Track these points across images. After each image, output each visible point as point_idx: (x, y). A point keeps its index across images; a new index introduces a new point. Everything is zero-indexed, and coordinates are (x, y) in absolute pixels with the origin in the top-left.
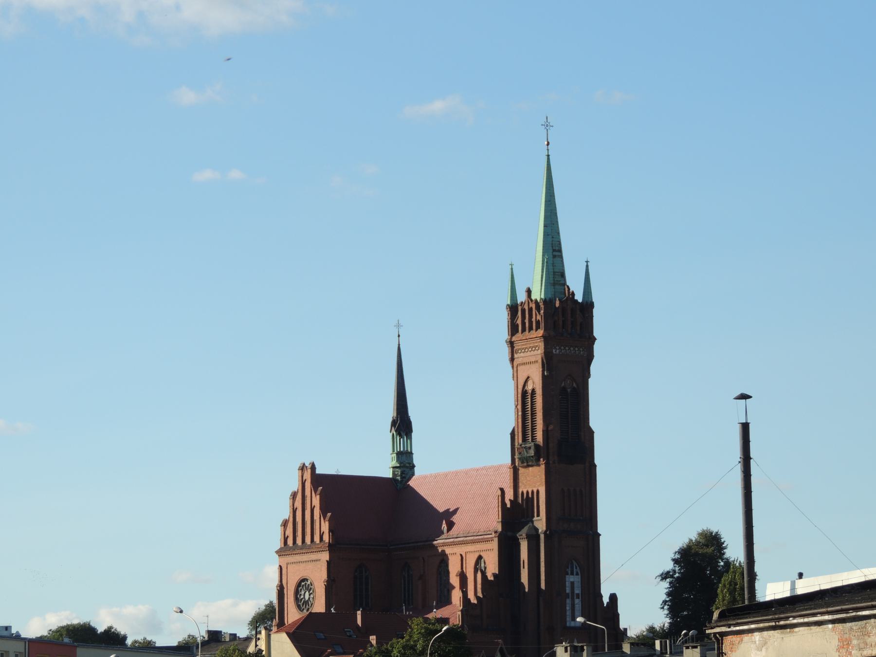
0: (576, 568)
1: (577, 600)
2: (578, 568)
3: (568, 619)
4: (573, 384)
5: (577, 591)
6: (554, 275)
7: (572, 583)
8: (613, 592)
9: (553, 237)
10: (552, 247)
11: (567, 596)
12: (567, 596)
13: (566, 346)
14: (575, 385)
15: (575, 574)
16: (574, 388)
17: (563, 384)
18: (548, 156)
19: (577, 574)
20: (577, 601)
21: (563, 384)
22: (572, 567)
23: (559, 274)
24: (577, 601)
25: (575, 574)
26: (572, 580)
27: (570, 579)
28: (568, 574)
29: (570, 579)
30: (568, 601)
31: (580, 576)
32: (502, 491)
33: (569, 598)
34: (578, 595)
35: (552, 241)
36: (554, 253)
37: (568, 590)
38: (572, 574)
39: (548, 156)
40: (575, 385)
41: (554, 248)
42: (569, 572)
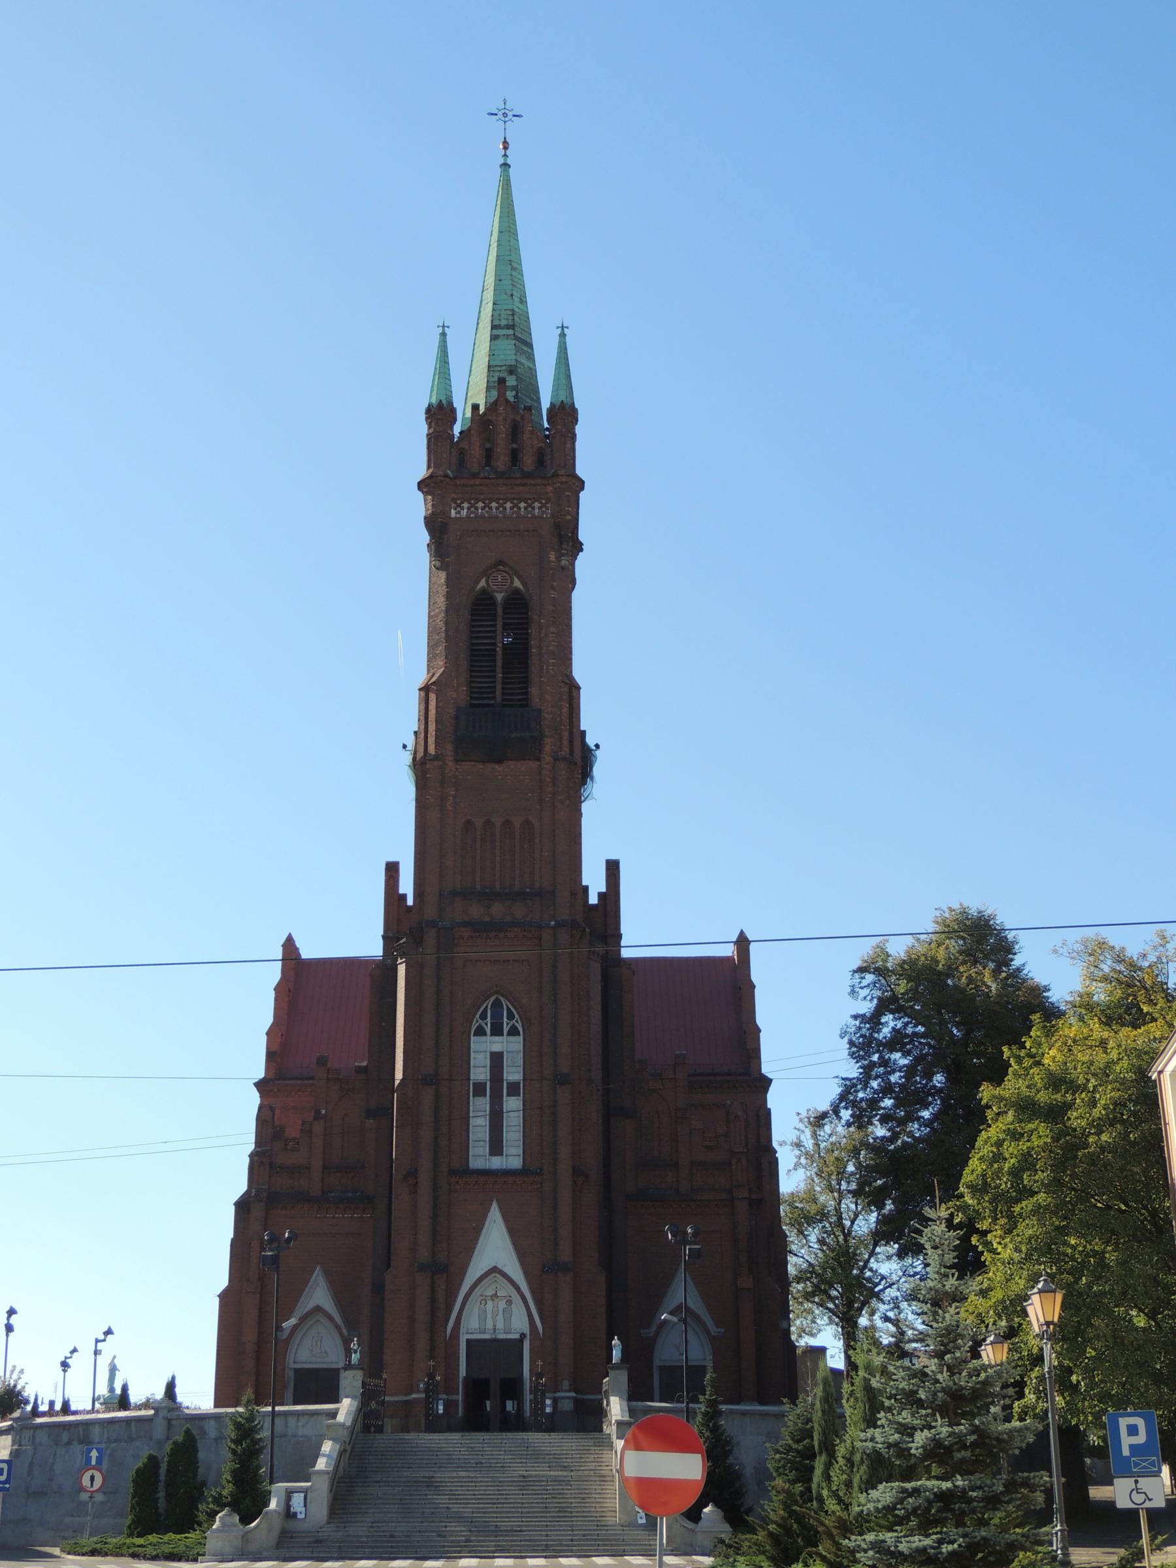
0: (511, 1017)
4: (512, 582)
5: (513, 1073)
7: (497, 1059)
14: (517, 583)
16: (517, 591)
17: (483, 583)
18: (506, 166)
19: (513, 1032)
20: (513, 1105)
21: (483, 583)
23: (504, 368)
24: (513, 1105)
25: (505, 1032)
26: (496, 1048)
28: (480, 1032)
29: (482, 1049)
31: (522, 1037)
32: (392, 869)
34: (514, 1089)
36: (496, 332)
37: (480, 1072)
38: (497, 1031)
39: (506, 166)
40: (517, 583)
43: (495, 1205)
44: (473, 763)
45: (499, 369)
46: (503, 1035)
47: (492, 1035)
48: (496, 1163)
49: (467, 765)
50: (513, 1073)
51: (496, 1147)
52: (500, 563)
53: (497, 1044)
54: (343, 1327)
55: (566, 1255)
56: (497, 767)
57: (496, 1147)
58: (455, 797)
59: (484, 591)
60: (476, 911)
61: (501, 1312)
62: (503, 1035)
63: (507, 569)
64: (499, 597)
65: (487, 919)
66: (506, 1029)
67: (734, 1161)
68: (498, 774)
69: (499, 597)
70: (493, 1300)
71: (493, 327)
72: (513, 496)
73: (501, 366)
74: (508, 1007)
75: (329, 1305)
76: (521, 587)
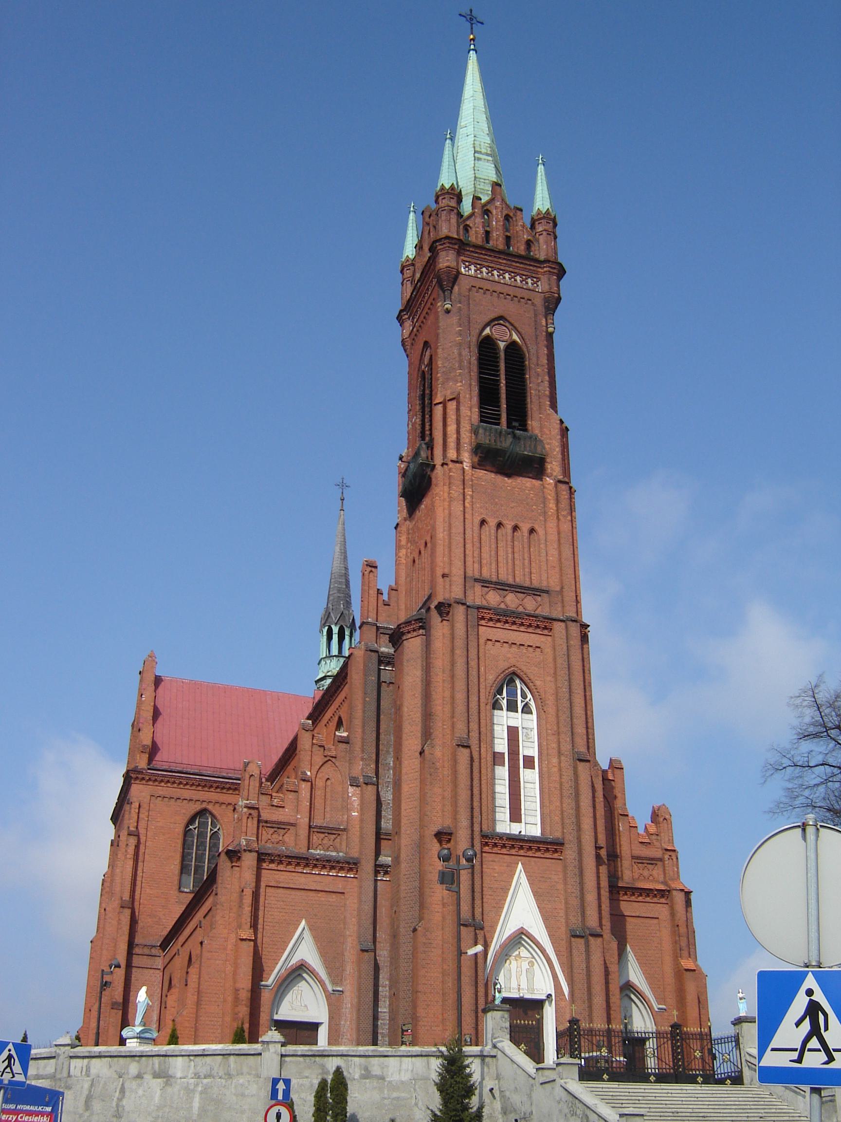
0: (524, 696)
1: (528, 771)
2: (529, 696)
3: (503, 815)
4: (511, 335)
5: (529, 748)
6: (475, 180)
7: (513, 733)
8: (657, 804)
9: (475, 136)
10: (474, 147)
11: (497, 759)
12: (497, 759)
13: (494, 269)
15: (520, 710)
16: (514, 343)
17: (487, 331)
19: (526, 710)
20: (530, 778)
21: (487, 331)
22: (512, 694)
24: (530, 778)
25: (520, 710)
27: (503, 720)
29: (503, 720)
30: (502, 772)
33: (503, 765)
34: (529, 762)
35: (474, 140)
36: (476, 155)
37: (501, 746)
38: (512, 707)
40: (515, 337)
41: (478, 149)
42: (504, 703)
43: (520, 866)
44: (485, 472)
45: (483, 181)
46: (517, 712)
47: (507, 710)
48: (515, 829)
49: (481, 473)
50: (529, 748)
51: (515, 816)
52: (501, 318)
53: (516, 719)
54: (327, 982)
55: (592, 921)
56: (506, 479)
57: (515, 816)
58: (472, 497)
59: (488, 337)
60: (493, 598)
61: (524, 972)
62: (517, 712)
63: (507, 324)
64: (502, 345)
65: (503, 606)
66: (520, 706)
67: (666, 857)
68: (506, 485)
69: (502, 345)
70: (516, 960)
71: (475, 152)
72: (511, 269)
73: (485, 179)
74: (521, 688)
75: (314, 960)
76: (518, 340)
